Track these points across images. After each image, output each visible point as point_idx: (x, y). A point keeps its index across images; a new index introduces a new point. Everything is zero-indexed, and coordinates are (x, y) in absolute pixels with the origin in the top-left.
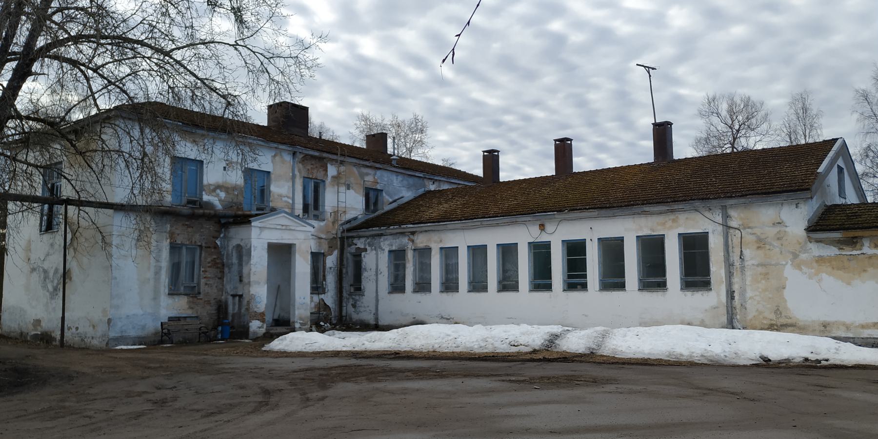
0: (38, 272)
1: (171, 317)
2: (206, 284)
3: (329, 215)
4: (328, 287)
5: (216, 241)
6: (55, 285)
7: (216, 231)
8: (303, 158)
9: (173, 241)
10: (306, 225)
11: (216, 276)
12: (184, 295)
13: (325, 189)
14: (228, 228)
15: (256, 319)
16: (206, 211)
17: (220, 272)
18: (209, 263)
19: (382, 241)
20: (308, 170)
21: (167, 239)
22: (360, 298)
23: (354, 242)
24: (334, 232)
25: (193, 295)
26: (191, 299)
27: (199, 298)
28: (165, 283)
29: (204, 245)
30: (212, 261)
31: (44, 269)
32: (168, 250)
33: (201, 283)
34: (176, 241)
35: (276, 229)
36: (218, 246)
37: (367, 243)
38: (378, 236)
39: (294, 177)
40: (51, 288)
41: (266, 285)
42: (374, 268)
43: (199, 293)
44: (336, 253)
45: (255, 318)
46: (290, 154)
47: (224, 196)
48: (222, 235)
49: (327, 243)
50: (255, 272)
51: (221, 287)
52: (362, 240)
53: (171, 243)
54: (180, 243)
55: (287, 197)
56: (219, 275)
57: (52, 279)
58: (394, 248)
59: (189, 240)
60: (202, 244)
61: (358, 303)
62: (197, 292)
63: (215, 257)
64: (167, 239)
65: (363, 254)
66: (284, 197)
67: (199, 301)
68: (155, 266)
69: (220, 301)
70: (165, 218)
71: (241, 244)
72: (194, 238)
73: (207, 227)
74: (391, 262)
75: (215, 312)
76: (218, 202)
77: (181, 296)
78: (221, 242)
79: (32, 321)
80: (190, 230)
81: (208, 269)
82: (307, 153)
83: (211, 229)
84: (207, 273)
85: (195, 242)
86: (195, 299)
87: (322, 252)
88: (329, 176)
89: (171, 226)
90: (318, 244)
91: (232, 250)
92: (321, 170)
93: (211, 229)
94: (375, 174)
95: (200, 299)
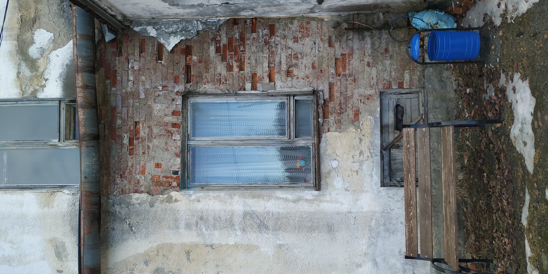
1: (383, 178)
2: (289, 73)
5: (170, 48)
9: (175, 179)
11: (267, 43)
12: (319, 142)
16: (80, 100)
17: (254, 30)
25: (321, 115)
26: (331, 119)
27: (327, 96)
28: (286, 200)
29: (180, 88)
30: (224, 59)
33: (286, 90)
34: (176, 173)
36: (181, 40)
43: (314, 93)
47: (43, 31)
48: (152, 32)
51: (295, 25)
54: (179, 160)
56: (263, 32)
59: (171, 134)
62: (311, 98)
63: (212, 49)
64: (170, 200)
67: (336, 94)
69: (337, 25)
70: (117, 208)
73: (131, 78)
75: (368, 40)
76: (59, 51)
77: (322, 151)
78: (170, 34)
80: (143, 133)
81: (247, 70)
83: (136, 68)
85: (174, 113)
86: (331, 105)
93: (136, 68)
95: (330, 89)
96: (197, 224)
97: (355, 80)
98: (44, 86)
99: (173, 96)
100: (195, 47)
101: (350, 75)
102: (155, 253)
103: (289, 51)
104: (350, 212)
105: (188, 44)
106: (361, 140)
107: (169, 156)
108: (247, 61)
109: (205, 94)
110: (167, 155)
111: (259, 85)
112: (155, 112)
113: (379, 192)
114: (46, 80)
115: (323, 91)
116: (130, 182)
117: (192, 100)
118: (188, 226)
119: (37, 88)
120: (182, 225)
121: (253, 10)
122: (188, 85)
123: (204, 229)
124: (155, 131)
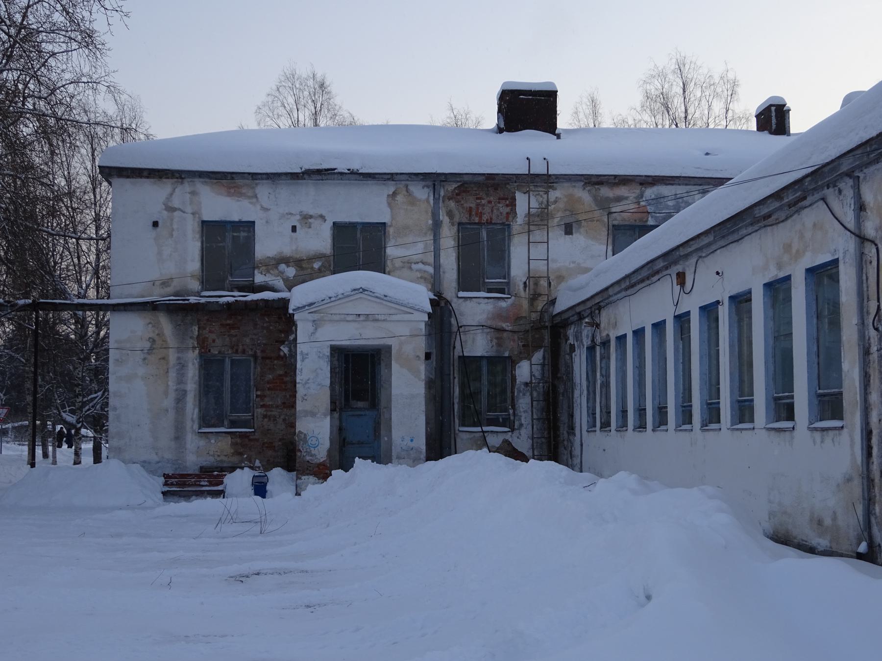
2: (265, 416)
3: (522, 286)
4: (520, 419)
5: (282, 348)
7: (281, 331)
8: (455, 188)
10: (411, 311)
13: (509, 239)
15: (308, 474)
18: (268, 383)
20: (470, 207)
21: (194, 348)
24: (534, 316)
26: (239, 440)
27: (251, 437)
28: (193, 414)
29: (259, 354)
32: (197, 366)
33: (255, 415)
35: (347, 321)
39: (437, 226)
41: (328, 418)
44: (538, 356)
45: (308, 471)
46: (428, 187)
48: (291, 338)
49: (516, 337)
50: (305, 395)
53: (201, 355)
55: (423, 263)
60: (255, 352)
63: (281, 372)
66: (418, 263)
67: (252, 443)
68: (176, 390)
70: (189, 318)
72: (241, 347)
80: (232, 331)
81: (268, 393)
82: (458, 179)
83: (271, 328)
84: (266, 399)
87: (507, 355)
88: (518, 216)
90: (495, 341)
92: (499, 205)
93: (271, 328)
94: (641, 196)
96: (180, 363)
97: (260, 453)
98: (262, 274)
99: (255, 349)
100: (282, 362)
101: (263, 450)
103: (278, 416)
104: (186, 450)
106: (226, 456)
108: (273, 392)
109: (255, 368)
111: (258, 399)
112: (245, 339)
113: (197, 465)
114: (265, 275)
115: (254, 435)
116: (205, 324)
117: (252, 359)
118: (179, 358)
119: (261, 269)
120: (180, 355)
122: (260, 358)
123: (177, 368)
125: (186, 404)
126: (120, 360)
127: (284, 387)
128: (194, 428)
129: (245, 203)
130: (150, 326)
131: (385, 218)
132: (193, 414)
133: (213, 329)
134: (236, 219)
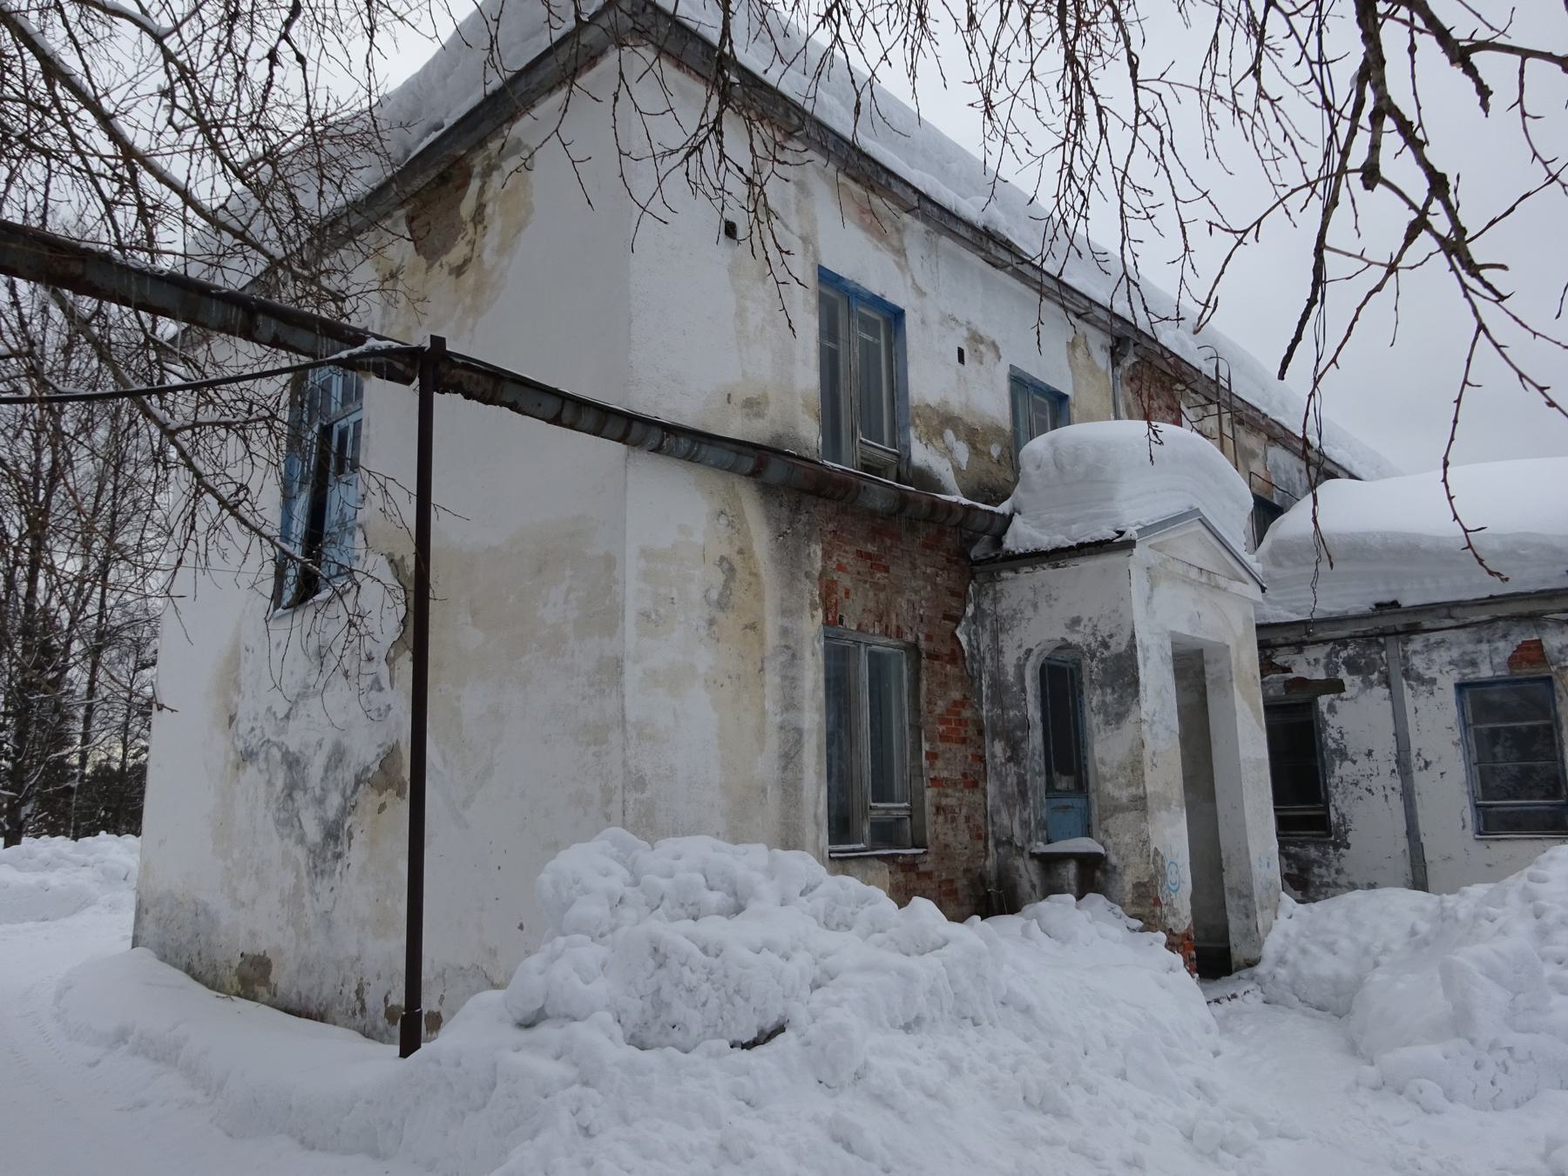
0: (263, 766)
5: (958, 633)
6: (331, 814)
14: (993, 578)
19: (1415, 652)
22: (1325, 854)
23: (1279, 660)
26: (900, 877)
27: (922, 868)
29: (923, 644)
31: (286, 754)
34: (841, 621)
37: (1340, 661)
38: (1397, 633)
40: (314, 833)
42: (1386, 746)
52: (1320, 652)
57: (318, 791)
58: (1486, 672)
61: (1316, 870)
63: (956, 695)
64: (814, 606)
65: (1323, 701)
71: (1075, 639)
72: (893, 616)
74: (1466, 726)
79: (236, 961)
89: (827, 555)
91: (1020, 668)
96: (787, 647)
102: (754, 571)
105: (960, 662)
107: (858, 613)
110: (859, 610)
118: (785, 632)
121: (1009, 760)
124: (882, 596)
125: (801, 771)
126: (653, 617)
127: (963, 735)
128: (821, 845)
129: (888, 259)
130: (723, 520)
131: (1066, 388)
132: (817, 803)
133: (845, 561)
134: (874, 286)
